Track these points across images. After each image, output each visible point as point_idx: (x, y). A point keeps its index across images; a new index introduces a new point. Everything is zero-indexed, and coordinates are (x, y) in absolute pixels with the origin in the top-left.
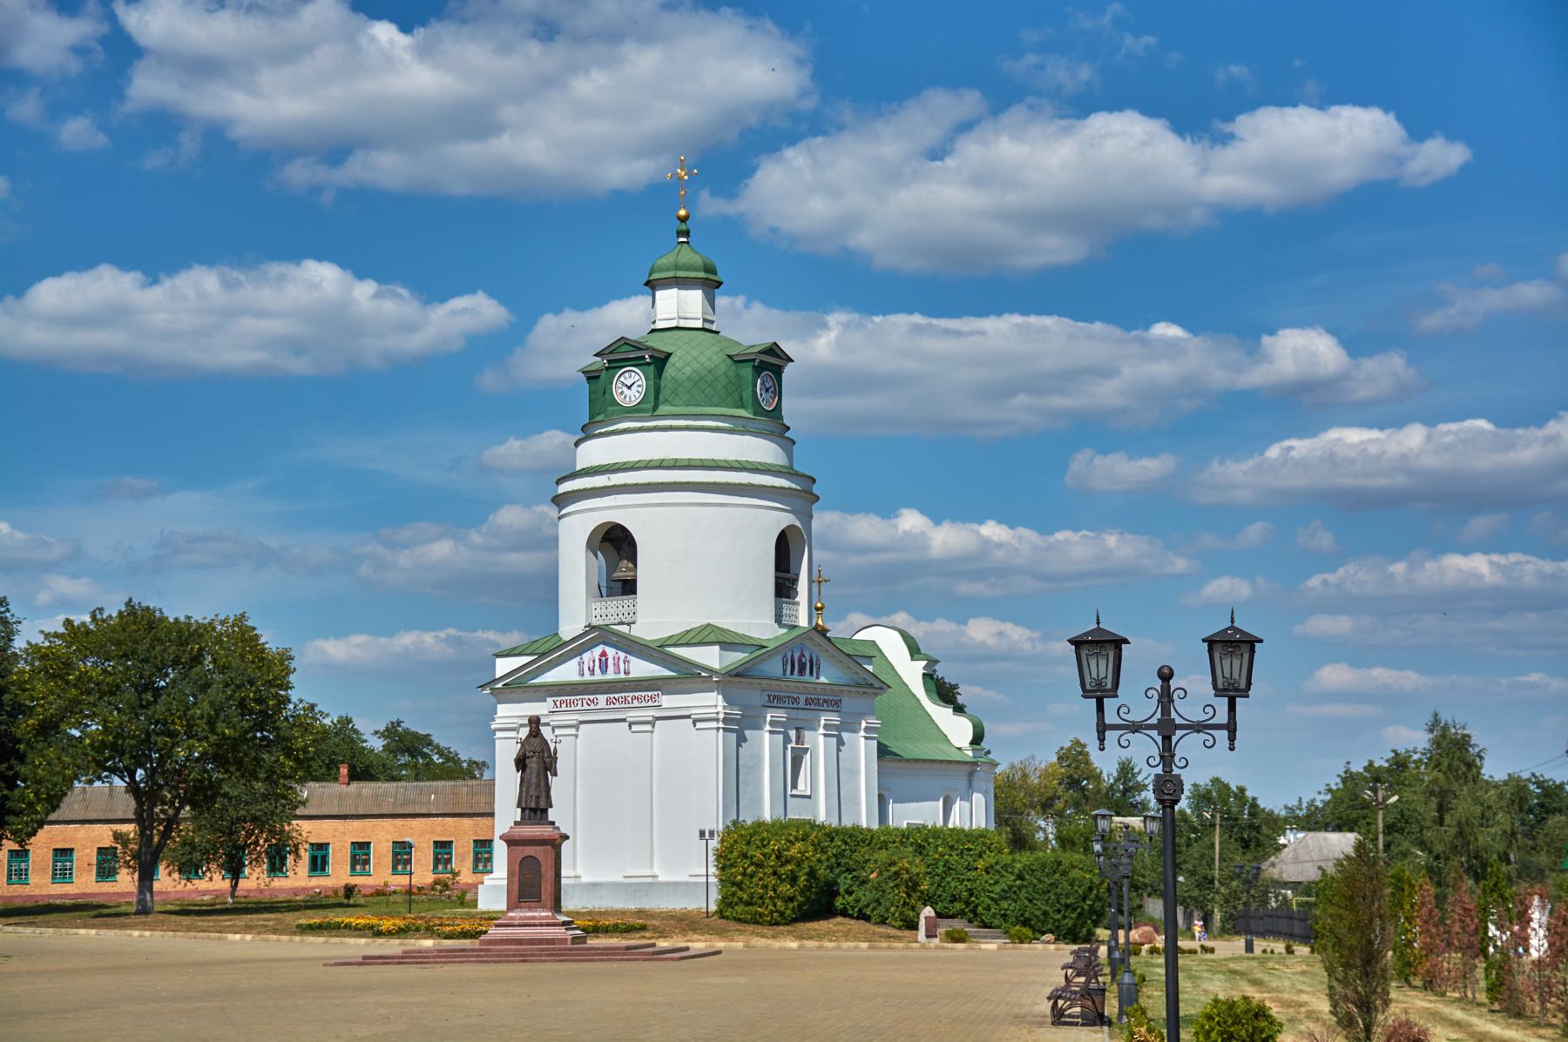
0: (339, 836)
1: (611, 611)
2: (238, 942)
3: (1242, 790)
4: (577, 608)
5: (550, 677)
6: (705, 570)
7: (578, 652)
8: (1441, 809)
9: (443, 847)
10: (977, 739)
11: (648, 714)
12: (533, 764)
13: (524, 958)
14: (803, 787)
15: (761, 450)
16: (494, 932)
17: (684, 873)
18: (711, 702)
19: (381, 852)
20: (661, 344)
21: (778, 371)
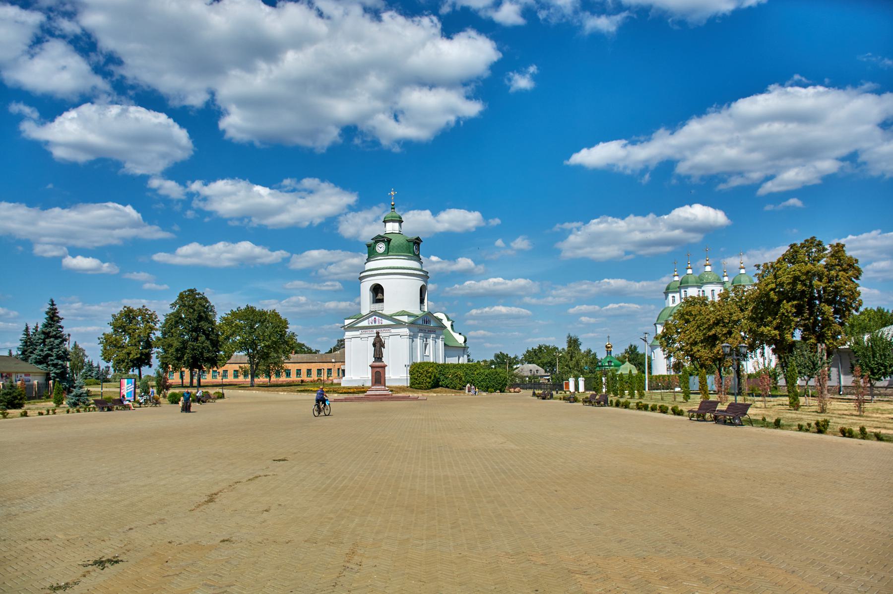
0: (293, 368)
1: (377, 306)
2: (283, 395)
5: (360, 325)
6: (402, 295)
7: (368, 318)
8: (571, 357)
9: (319, 371)
10: (465, 341)
11: (388, 334)
12: (378, 345)
13: (382, 400)
14: (427, 353)
15: (414, 264)
16: (368, 393)
18: (406, 331)
20: (389, 236)
21: (419, 244)
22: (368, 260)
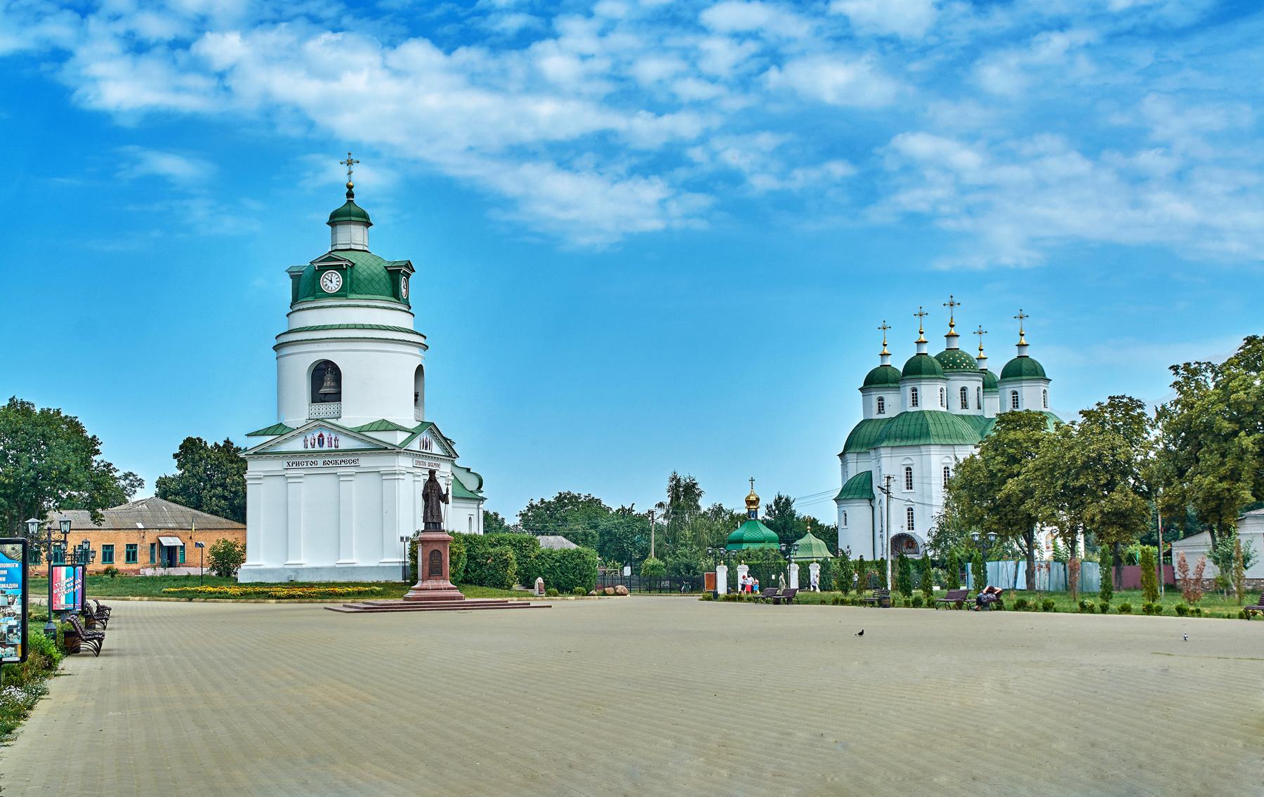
1: (325, 409)
3: (496, 514)
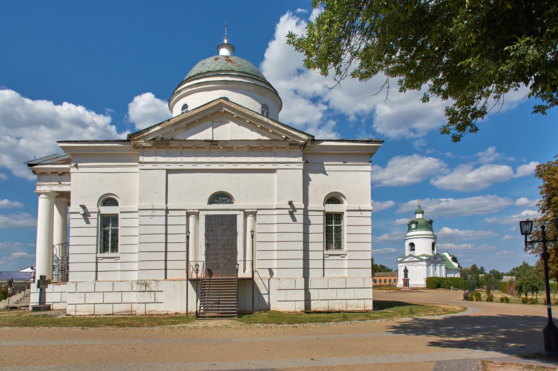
1: (412, 253)
4: (408, 252)
6: (423, 247)
10: (459, 266)
17: (422, 283)
18: (425, 263)
19: (383, 280)
20: (417, 221)
22: (408, 232)
